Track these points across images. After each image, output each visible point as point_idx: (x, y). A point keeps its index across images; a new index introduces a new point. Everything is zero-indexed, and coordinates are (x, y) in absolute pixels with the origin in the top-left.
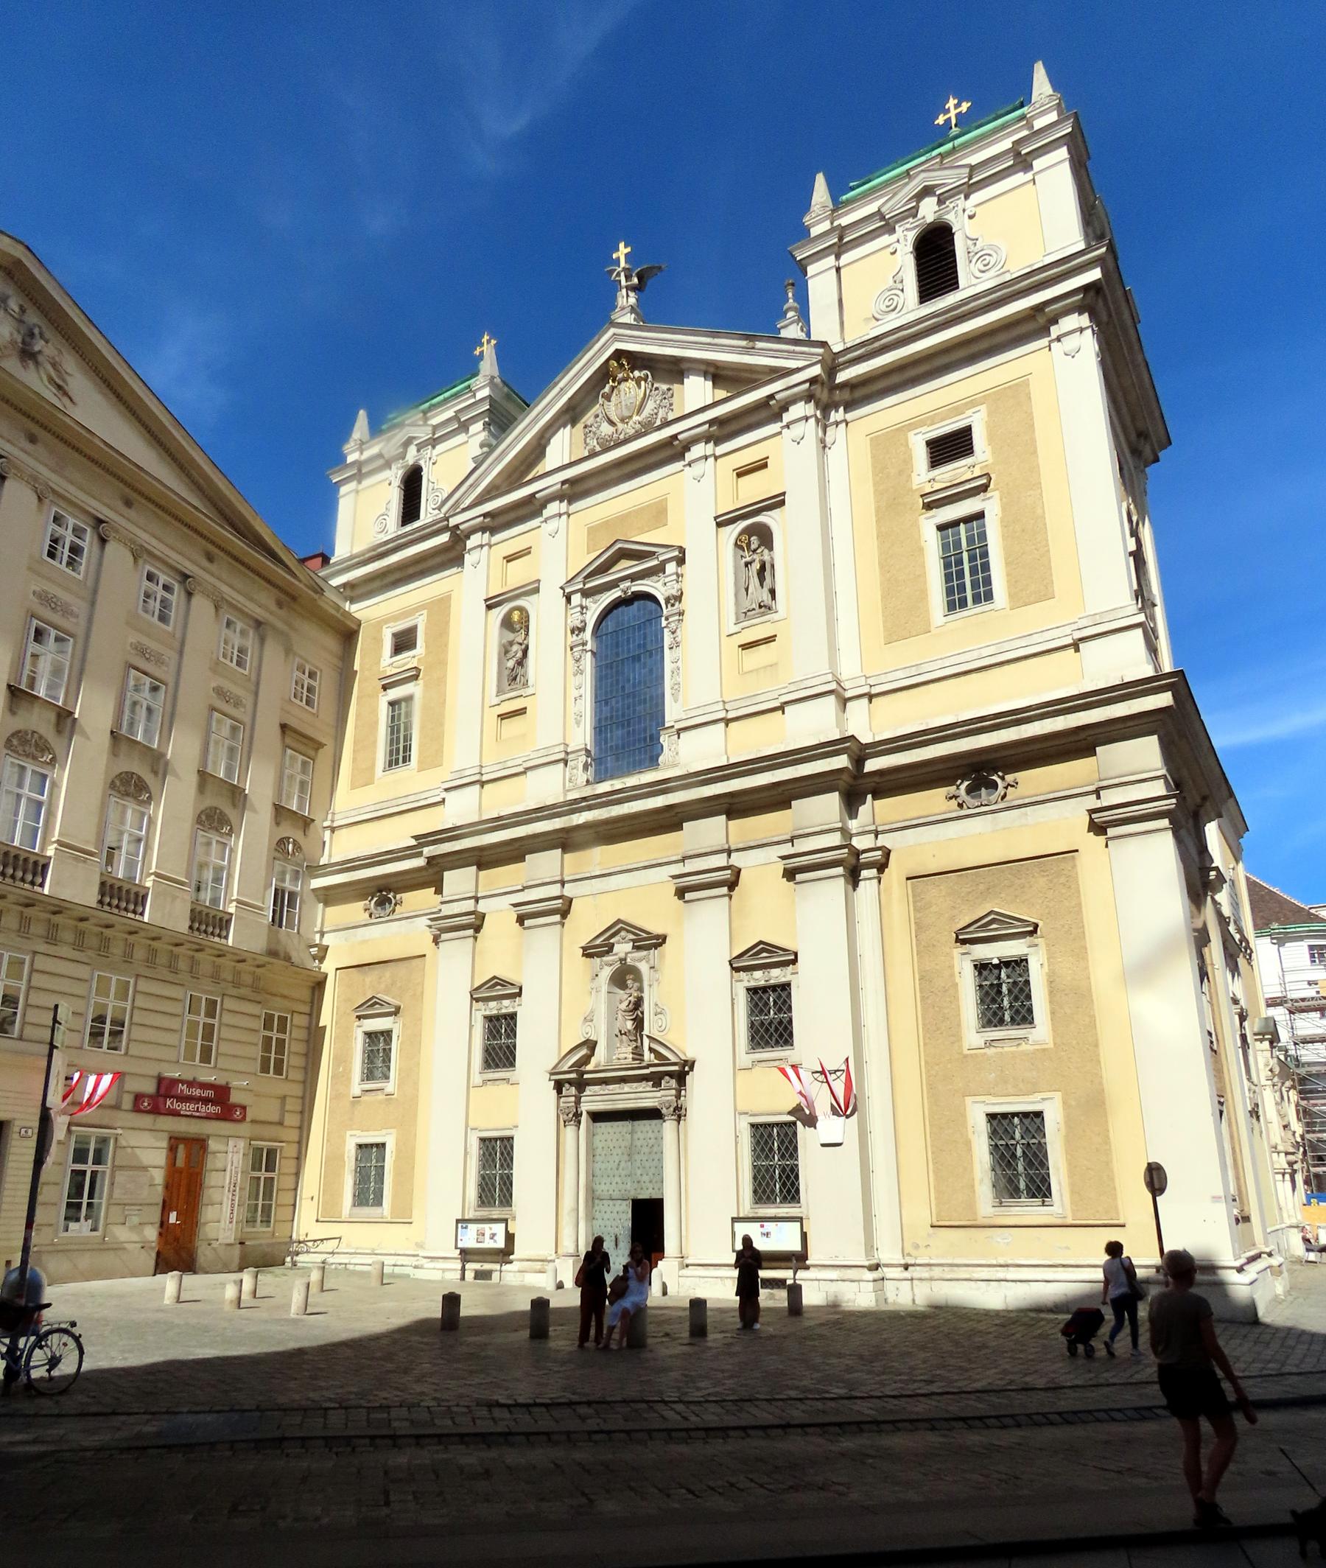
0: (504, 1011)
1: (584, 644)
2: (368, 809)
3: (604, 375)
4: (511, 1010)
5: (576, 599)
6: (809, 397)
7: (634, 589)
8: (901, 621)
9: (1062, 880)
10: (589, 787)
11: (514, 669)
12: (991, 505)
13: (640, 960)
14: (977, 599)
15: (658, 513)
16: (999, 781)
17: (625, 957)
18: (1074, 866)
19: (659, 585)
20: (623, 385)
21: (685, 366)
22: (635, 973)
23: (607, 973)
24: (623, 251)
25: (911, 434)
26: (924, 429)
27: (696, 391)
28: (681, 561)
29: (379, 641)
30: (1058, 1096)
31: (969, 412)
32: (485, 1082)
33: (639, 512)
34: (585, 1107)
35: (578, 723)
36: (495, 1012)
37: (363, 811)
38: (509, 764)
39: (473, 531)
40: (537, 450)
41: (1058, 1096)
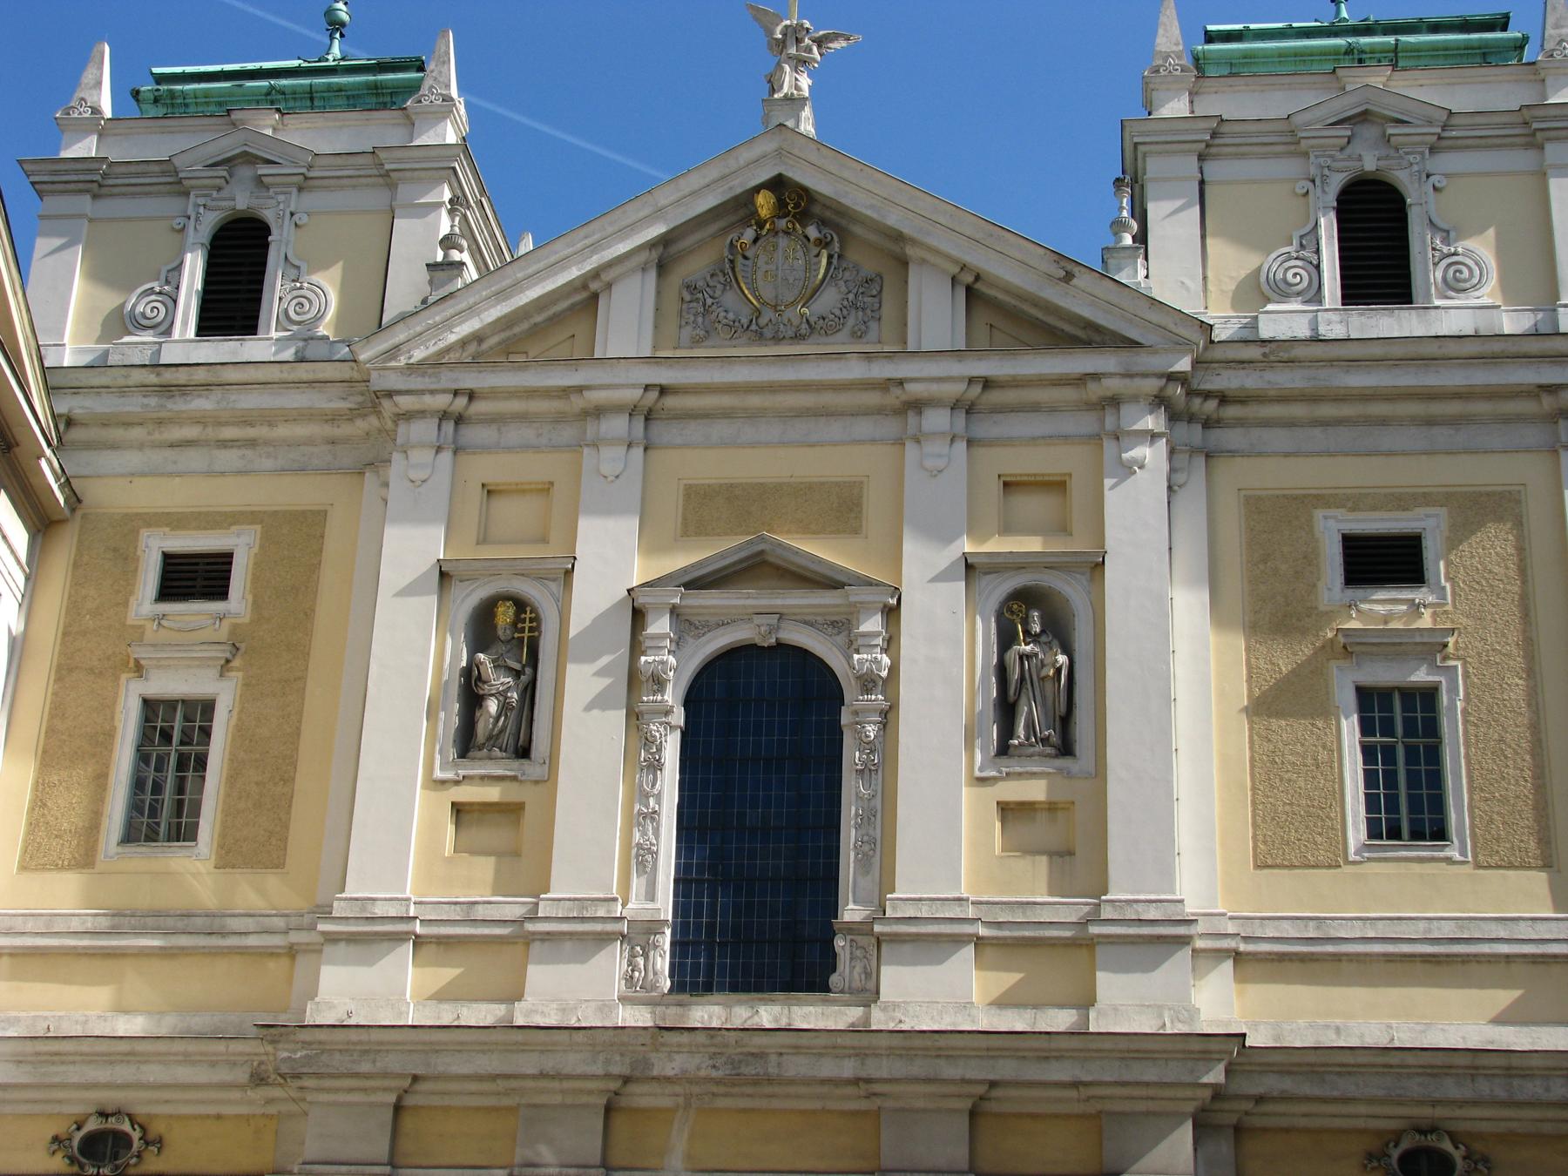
1: (667, 713)
5: (660, 625)
6: (1160, 401)
8: (1283, 834)
11: (496, 717)
14: (1417, 835)
20: (783, 241)
21: (910, 251)
25: (1319, 514)
28: (892, 613)
29: (127, 560)
33: (803, 492)
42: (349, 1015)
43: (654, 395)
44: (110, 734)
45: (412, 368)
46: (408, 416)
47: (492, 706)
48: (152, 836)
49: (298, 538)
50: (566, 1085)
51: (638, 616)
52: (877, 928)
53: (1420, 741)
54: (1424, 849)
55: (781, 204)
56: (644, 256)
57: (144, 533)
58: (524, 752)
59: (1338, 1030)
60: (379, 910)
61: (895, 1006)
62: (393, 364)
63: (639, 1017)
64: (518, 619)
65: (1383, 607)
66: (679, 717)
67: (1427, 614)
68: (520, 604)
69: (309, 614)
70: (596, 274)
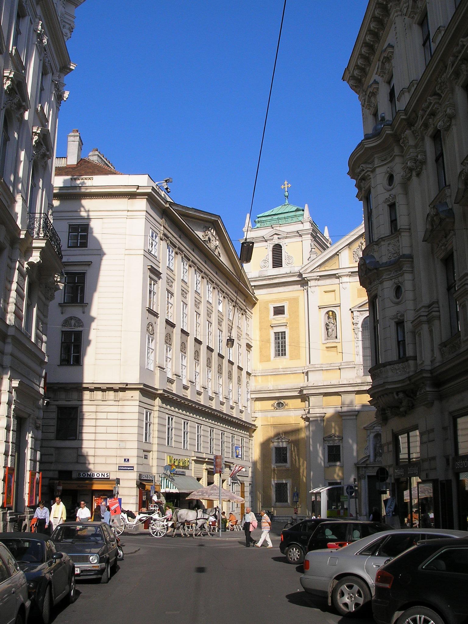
2: (269, 371)
4: (338, 444)
5: (356, 313)
23: (372, 435)
29: (267, 309)
36: (332, 445)
37: (267, 371)
44: (269, 339)
46: (309, 280)
47: (330, 330)
48: (279, 355)
49: (295, 301)
51: (352, 312)
57: (270, 304)
58: (337, 338)
60: (316, 366)
63: (359, 381)
64: (333, 315)
66: (361, 329)
68: (333, 312)
69: (298, 316)
70: (338, 252)
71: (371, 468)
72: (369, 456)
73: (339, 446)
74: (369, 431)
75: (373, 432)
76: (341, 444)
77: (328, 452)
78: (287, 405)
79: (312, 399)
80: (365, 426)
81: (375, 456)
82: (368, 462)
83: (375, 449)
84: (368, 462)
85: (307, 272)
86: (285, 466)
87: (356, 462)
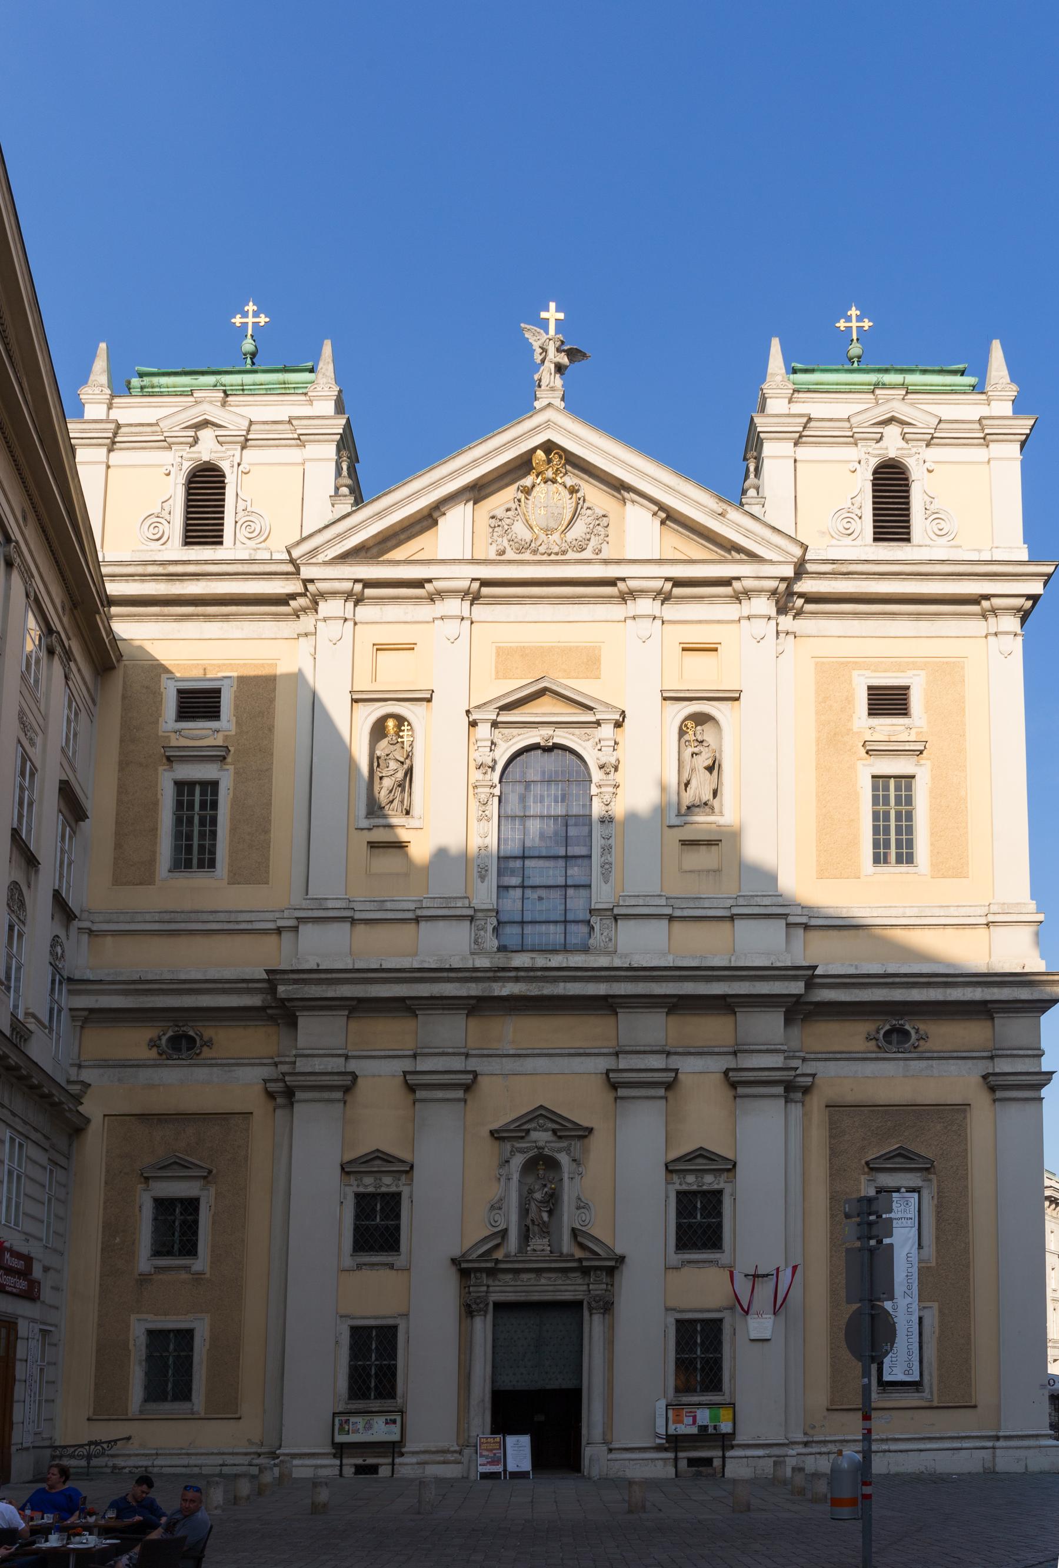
0: (384, 1189)
3: (522, 465)
4: (393, 1189)
7: (556, 740)
9: (955, 1128)
10: (500, 955)
12: (924, 774)
13: (559, 1151)
15: (590, 661)
16: (913, 1032)
17: (541, 1151)
18: (965, 1118)
19: (589, 744)
22: (553, 1164)
24: (552, 314)
26: (868, 673)
27: (638, 534)
28: (618, 725)
30: (935, 1305)
31: (910, 673)
32: (360, 1267)
34: (494, 1297)
35: (482, 878)
36: (371, 1189)
38: (389, 906)
39: (334, 594)
40: (427, 520)
41: (935, 1305)
42: (318, 965)
43: (476, 585)
45: (325, 563)
50: (444, 1002)
52: (616, 911)
53: (904, 808)
54: (904, 868)
55: (549, 461)
56: (467, 495)
59: (856, 968)
60: (330, 904)
61: (626, 956)
62: (314, 560)
65: (887, 727)
67: (913, 731)
71: (508, 1277)
72: (504, 1233)
73: (396, 1197)
74: (508, 1146)
75: (522, 1151)
76: (405, 1191)
77: (357, 1217)
78: (209, 1043)
79: (305, 1022)
80: (495, 1126)
81: (525, 1236)
82: (499, 1255)
83: (524, 1212)
84: (499, 1255)
85: (321, 558)
86: (187, 1268)
87: (457, 1253)
